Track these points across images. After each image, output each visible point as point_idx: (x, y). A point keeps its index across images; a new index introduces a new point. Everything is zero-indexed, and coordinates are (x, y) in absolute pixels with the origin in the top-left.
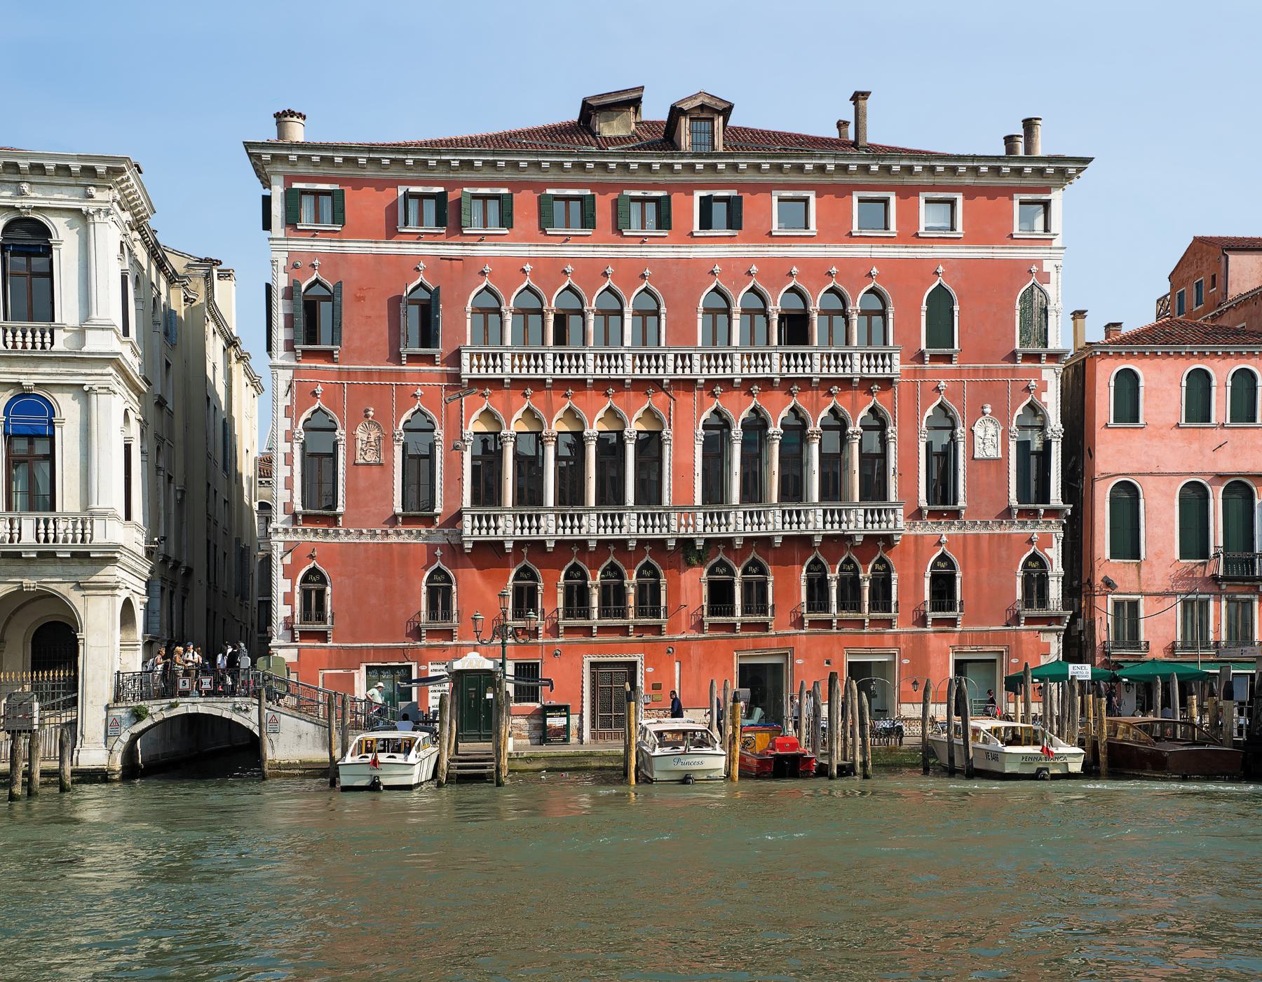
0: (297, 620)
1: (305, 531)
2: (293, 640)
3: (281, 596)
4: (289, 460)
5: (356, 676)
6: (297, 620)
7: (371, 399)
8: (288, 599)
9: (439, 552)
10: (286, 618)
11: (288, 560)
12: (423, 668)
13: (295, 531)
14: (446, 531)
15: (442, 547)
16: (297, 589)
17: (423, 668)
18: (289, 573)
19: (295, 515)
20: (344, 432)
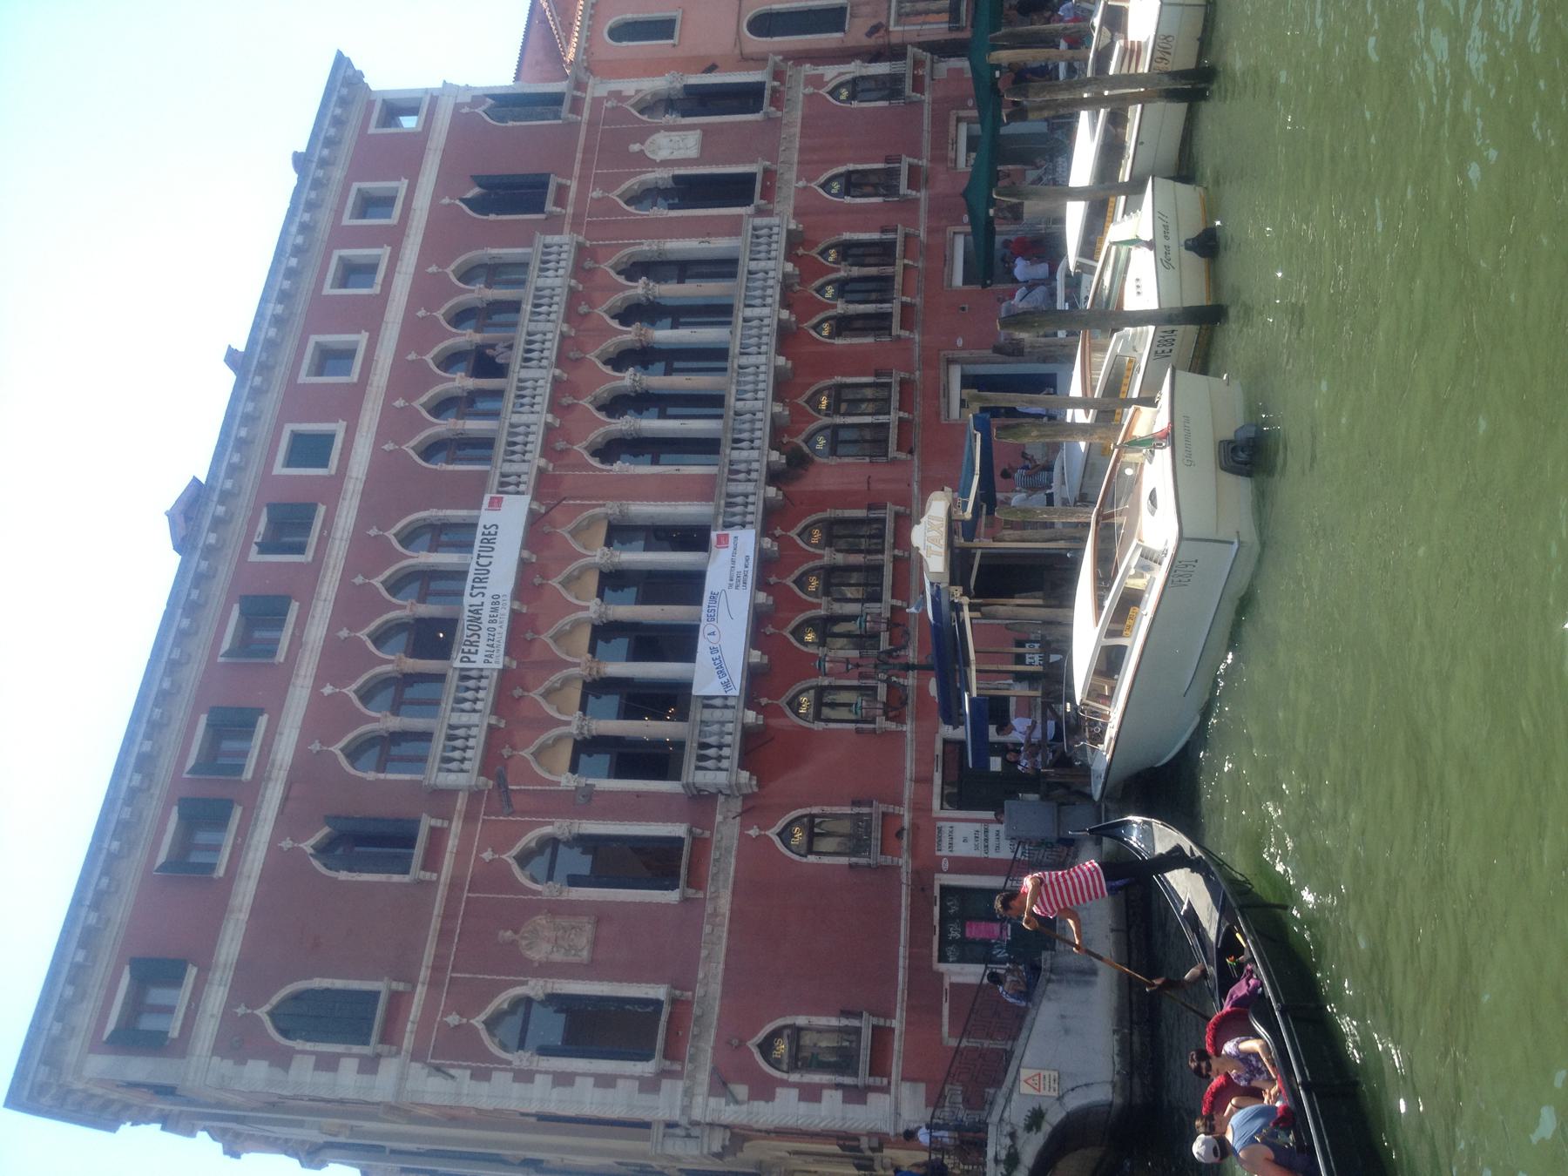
0: (847, 1080)
1: (693, 1059)
2: (885, 1090)
3: (804, 1107)
4: (564, 1079)
5: (955, 979)
6: (847, 1080)
7: (485, 929)
8: (811, 1094)
9: (754, 832)
10: (846, 1100)
11: (741, 1090)
12: (945, 865)
13: (692, 1077)
14: (719, 818)
15: (744, 826)
16: (795, 1077)
17: (945, 865)
18: (764, 1090)
19: (663, 1074)
20: (532, 982)
